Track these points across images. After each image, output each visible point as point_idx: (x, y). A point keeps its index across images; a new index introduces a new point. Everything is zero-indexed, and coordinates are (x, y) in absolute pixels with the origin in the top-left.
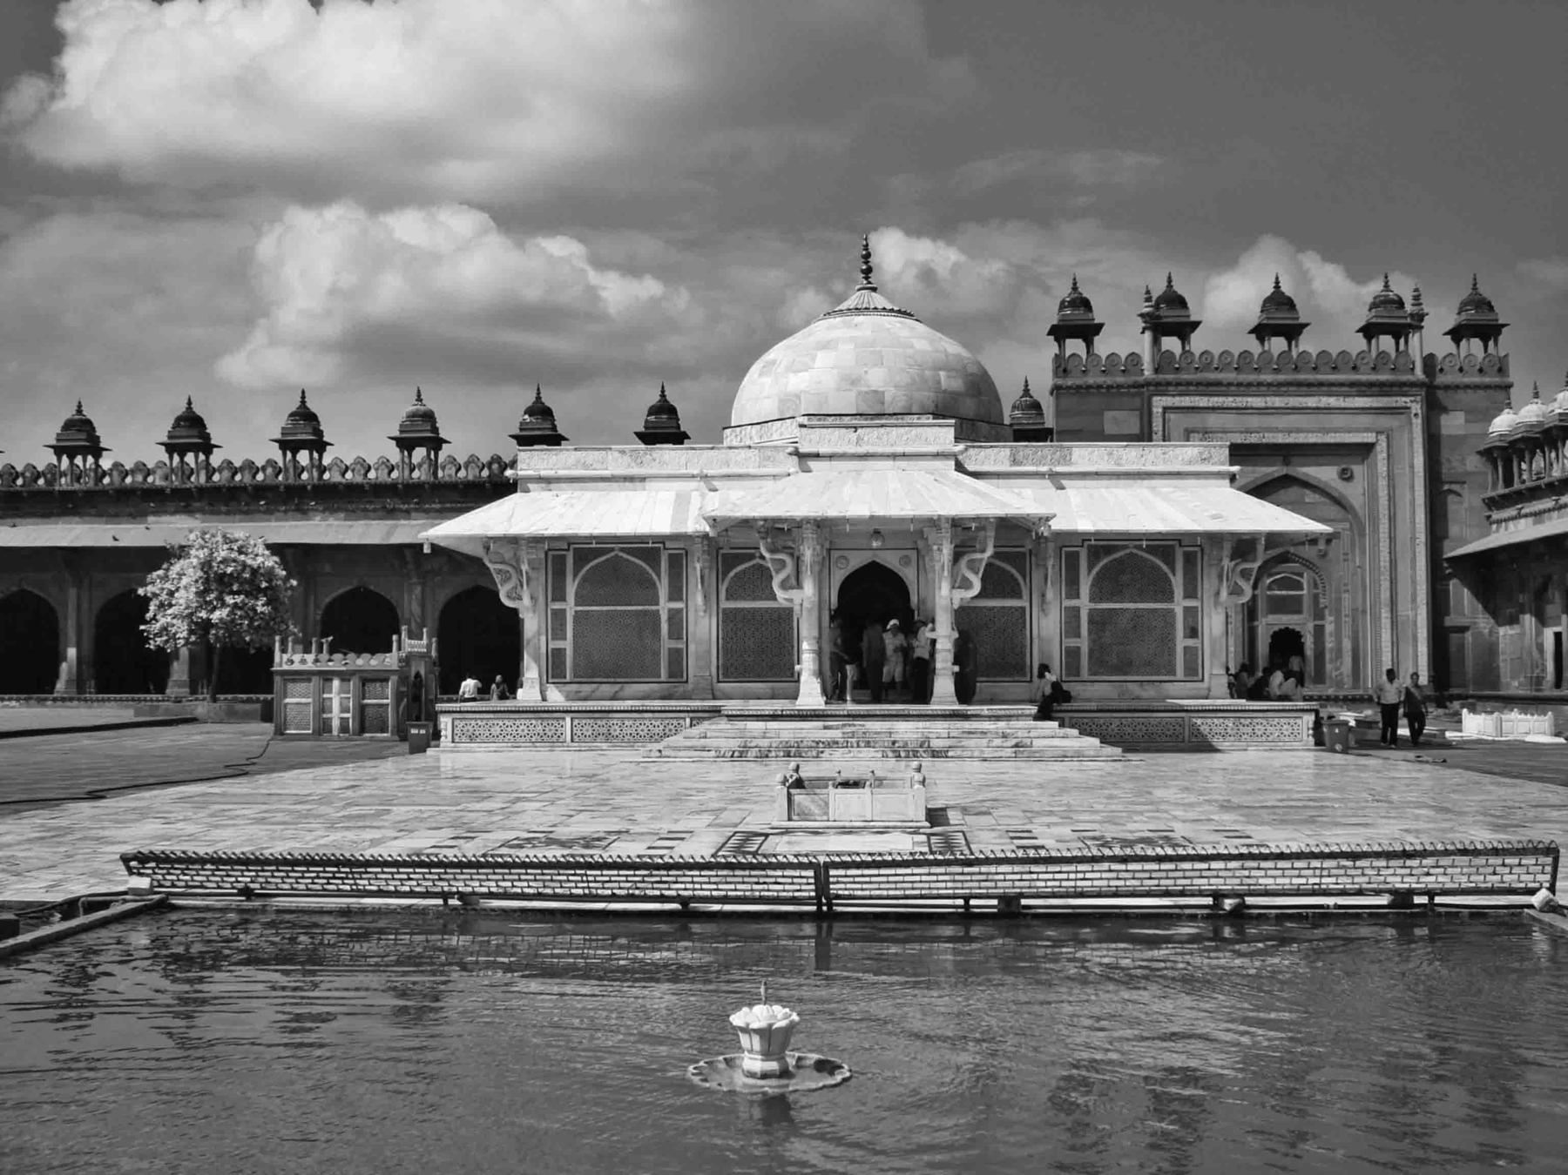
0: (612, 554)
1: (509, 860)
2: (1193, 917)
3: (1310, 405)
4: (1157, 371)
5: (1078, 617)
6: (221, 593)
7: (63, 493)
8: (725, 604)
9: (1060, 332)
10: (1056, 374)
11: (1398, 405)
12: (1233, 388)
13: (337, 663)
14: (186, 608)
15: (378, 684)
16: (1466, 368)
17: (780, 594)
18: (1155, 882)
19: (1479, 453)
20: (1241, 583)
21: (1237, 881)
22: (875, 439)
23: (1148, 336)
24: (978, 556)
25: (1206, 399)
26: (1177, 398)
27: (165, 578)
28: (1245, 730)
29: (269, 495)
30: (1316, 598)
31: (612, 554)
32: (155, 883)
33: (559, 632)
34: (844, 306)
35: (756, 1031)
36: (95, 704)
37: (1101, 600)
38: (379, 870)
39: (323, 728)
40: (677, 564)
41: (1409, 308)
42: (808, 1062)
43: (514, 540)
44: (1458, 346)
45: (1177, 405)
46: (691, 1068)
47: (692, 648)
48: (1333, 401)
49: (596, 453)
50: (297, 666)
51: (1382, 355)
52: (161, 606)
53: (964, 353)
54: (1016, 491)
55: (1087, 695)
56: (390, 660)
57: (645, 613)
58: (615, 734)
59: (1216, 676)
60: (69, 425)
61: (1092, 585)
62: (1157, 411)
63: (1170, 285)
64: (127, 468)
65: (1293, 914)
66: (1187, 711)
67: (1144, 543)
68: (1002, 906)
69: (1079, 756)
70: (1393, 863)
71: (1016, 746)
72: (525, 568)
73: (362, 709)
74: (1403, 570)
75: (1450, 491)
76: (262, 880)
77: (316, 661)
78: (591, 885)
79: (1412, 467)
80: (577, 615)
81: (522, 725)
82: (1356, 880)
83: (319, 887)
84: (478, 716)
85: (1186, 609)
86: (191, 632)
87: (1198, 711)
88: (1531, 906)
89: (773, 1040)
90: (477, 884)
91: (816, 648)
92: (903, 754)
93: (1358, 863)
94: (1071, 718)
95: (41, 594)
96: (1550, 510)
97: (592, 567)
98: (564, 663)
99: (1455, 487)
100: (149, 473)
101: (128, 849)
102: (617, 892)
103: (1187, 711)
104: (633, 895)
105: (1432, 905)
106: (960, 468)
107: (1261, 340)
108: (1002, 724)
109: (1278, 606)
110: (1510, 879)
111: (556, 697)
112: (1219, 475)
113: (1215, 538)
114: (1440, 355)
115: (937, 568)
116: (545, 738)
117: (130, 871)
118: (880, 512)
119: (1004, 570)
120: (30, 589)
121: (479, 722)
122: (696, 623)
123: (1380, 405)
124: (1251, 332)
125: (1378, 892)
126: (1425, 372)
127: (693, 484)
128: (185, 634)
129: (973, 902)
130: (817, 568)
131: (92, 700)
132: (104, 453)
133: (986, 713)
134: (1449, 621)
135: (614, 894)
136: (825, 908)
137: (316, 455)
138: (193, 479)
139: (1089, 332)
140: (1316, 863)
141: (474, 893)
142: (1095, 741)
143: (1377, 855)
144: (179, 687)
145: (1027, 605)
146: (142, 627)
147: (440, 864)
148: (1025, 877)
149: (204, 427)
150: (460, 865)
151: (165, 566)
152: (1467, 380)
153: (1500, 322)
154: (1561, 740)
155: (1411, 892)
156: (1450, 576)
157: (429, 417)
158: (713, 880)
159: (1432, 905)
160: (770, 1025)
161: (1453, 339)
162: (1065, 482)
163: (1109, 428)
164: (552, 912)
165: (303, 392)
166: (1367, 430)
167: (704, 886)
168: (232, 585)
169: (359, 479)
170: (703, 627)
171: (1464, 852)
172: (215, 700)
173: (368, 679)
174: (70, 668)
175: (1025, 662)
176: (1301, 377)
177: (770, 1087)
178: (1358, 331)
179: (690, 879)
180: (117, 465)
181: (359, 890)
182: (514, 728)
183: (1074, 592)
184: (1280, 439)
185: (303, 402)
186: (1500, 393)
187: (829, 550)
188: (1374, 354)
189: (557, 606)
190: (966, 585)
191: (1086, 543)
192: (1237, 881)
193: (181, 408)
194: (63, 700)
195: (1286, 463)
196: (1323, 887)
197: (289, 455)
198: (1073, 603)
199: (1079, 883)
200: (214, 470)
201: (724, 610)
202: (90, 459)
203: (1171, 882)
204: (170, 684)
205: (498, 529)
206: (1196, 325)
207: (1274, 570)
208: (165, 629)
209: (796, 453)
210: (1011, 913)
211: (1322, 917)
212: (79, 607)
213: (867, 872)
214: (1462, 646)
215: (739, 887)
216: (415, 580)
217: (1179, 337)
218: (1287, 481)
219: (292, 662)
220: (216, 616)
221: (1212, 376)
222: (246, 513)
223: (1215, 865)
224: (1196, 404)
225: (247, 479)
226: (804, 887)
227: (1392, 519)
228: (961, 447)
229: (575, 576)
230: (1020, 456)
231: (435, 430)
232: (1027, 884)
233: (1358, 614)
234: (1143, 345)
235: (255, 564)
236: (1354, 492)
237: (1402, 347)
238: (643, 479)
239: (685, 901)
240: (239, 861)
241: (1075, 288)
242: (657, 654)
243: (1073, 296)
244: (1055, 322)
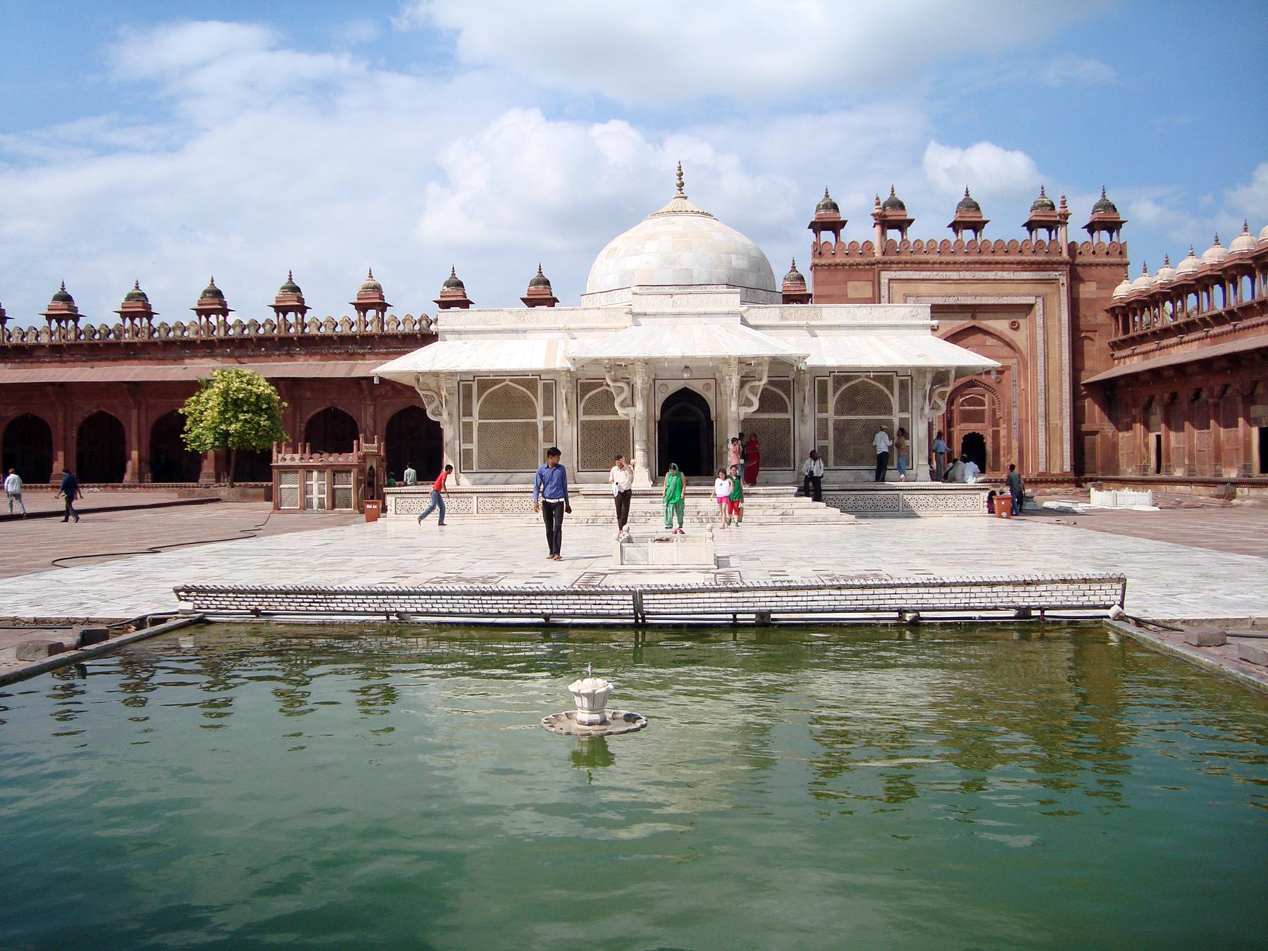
0: (504, 384)
1: (430, 590)
2: (886, 625)
3: (989, 277)
4: (884, 254)
6: (236, 412)
7: (129, 346)
8: (582, 418)
9: (817, 227)
10: (814, 256)
11: (1051, 277)
12: (938, 266)
13: (316, 460)
14: (212, 423)
15: (344, 475)
16: (1097, 251)
17: (620, 411)
18: (860, 602)
19: (1107, 311)
20: (940, 402)
21: (915, 601)
22: (685, 302)
23: (878, 228)
24: (757, 383)
25: (918, 273)
26: (898, 273)
27: (197, 403)
28: (941, 503)
29: (268, 343)
30: (994, 411)
31: (504, 384)
32: (196, 606)
33: (467, 437)
34: (664, 210)
35: (583, 694)
36: (151, 489)
37: (842, 414)
38: (344, 597)
39: (307, 505)
40: (549, 389)
41: (1058, 209)
42: (620, 716)
43: (436, 374)
44: (1092, 236)
45: (898, 277)
46: (543, 719)
48: (1006, 275)
49: (493, 313)
50: (288, 463)
51: (1040, 242)
52: (195, 422)
53: (749, 242)
54: (784, 338)
55: (831, 479)
56: (351, 458)
58: (507, 508)
59: (921, 465)
60: (130, 297)
62: (884, 281)
63: (893, 194)
64: (171, 326)
65: (951, 624)
66: (901, 490)
67: (872, 374)
68: (759, 619)
69: (825, 521)
70: (1017, 589)
72: (444, 393)
73: (334, 491)
74: (1054, 392)
75: (1086, 337)
76: (267, 604)
77: (302, 458)
78: (484, 606)
79: (1060, 320)
80: (481, 426)
82: (994, 600)
83: (304, 608)
84: (412, 496)
86: (216, 439)
87: (912, 490)
88: (1108, 617)
89: (596, 701)
90: (409, 605)
91: (644, 447)
92: (704, 520)
93: (995, 589)
95: (112, 413)
96: (1153, 351)
99: (1089, 334)
100: (185, 329)
101: (180, 584)
102: (501, 610)
103: (901, 490)
104: (512, 613)
105: (1043, 617)
106: (744, 322)
107: (956, 231)
108: (774, 499)
109: (968, 417)
110: (1095, 600)
111: (466, 483)
112: (924, 326)
113: (921, 371)
114: (1079, 242)
115: (728, 392)
117: (179, 597)
118: (689, 353)
119: (776, 394)
120: (102, 409)
123: (1038, 278)
124: (948, 227)
125: (1007, 608)
126: (1069, 254)
127: (560, 335)
128: (212, 440)
129: (738, 616)
130: (645, 393)
131: (149, 487)
132: (154, 316)
133: (762, 492)
134: (1085, 428)
135: (500, 613)
136: (640, 621)
137: (299, 316)
138: (215, 333)
139: (836, 226)
140: (966, 589)
141: (407, 612)
142: (838, 510)
143: (1008, 583)
144: (208, 477)
146: (182, 436)
147: (383, 593)
148: (773, 599)
149: (223, 297)
150: (397, 593)
151: (197, 394)
152: (1098, 260)
153: (1121, 220)
154: (1157, 509)
155: (1029, 608)
156: (1085, 397)
157: (377, 288)
158: (565, 602)
159: (1043, 617)
160: (594, 691)
161: (1089, 231)
162: (817, 332)
163: (851, 294)
164: (458, 624)
166: (1029, 295)
167: (560, 607)
168: (243, 406)
169: (330, 332)
170: (567, 437)
171: (1064, 581)
172: (233, 486)
173: (337, 471)
174: (134, 464)
175: (789, 457)
176: (984, 258)
177: (594, 730)
178: (1024, 226)
179: (550, 602)
180: (163, 324)
181: (330, 611)
184: (969, 301)
185: (291, 279)
186: (1119, 266)
188: (1034, 242)
189: (467, 419)
191: (832, 374)
192: (915, 601)
193: (206, 286)
194: (129, 487)
195: (974, 317)
196: (971, 605)
197: (281, 315)
198: (824, 415)
199: (809, 603)
200: (230, 327)
202: (145, 320)
203: (871, 602)
204: (202, 475)
205: (425, 368)
207: (966, 392)
208: (197, 437)
209: (631, 313)
210: (764, 622)
211: (971, 625)
212: (139, 424)
213: (667, 596)
214: (1094, 443)
215: (582, 607)
216: (369, 403)
218: (974, 330)
219: (285, 460)
220: (232, 428)
221: (923, 257)
222: (252, 357)
223: (899, 590)
224: (911, 277)
225: (253, 333)
226: (626, 607)
227: (1046, 357)
228: (745, 307)
230: (786, 314)
231: (382, 297)
232: (774, 604)
233: (1022, 423)
234: (873, 234)
235: (258, 392)
236: (1020, 338)
237: (1053, 237)
238: (525, 331)
239: (547, 617)
240: (251, 592)
242: (535, 453)
243: (826, 202)
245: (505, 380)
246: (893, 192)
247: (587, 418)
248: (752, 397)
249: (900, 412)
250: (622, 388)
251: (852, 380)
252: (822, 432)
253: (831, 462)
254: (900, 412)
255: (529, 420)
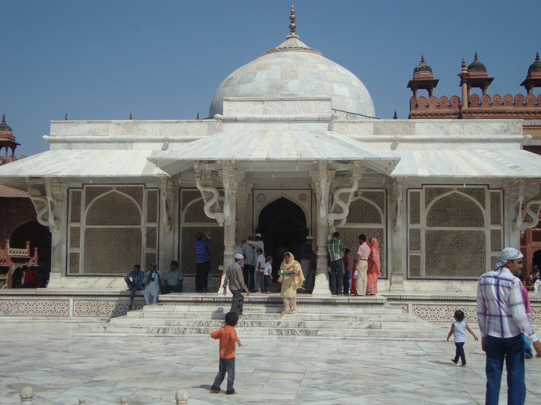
5: (419, 235)
8: (184, 225)
9: (414, 85)
20: (531, 214)
33: (75, 243)
37: (434, 225)
40: (153, 197)
47: (162, 253)
57: (132, 230)
58: (102, 311)
61: (429, 215)
71: (370, 327)
72: (49, 198)
80: (88, 231)
81: (40, 304)
85: (493, 231)
92: (283, 332)
94: (413, 305)
97: (98, 200)
98: (78, 263)
107: (528, 88)
116: (56, 314)
118: (275, 156)
119: (369, 205)
121: (11, 302)
122: (164, 236)
124: (522, 85)
145: (384, 227)
165: (4, 116)
182: (35, 306)
183: (415, 219)
187: (253, 190)
189: (75, 225)
190: (339, 210)
191: (424, 187)
201: (184, 229)
206: (490, 80)
217: (481, 88)
229: (87, 205)
238: (132, 141)
241: (423, 61)
243: (421, 65)
244: (411, 79)
245: (112, 188)
246: (476, 57)
247: (188, 225)
248: (341, 204)
249: (493, 222)
250: (211, 193)
251: (444, 192)
252: (414, 244)
253: (423, 274)
254: (493, 222)
255: (132, 226)
